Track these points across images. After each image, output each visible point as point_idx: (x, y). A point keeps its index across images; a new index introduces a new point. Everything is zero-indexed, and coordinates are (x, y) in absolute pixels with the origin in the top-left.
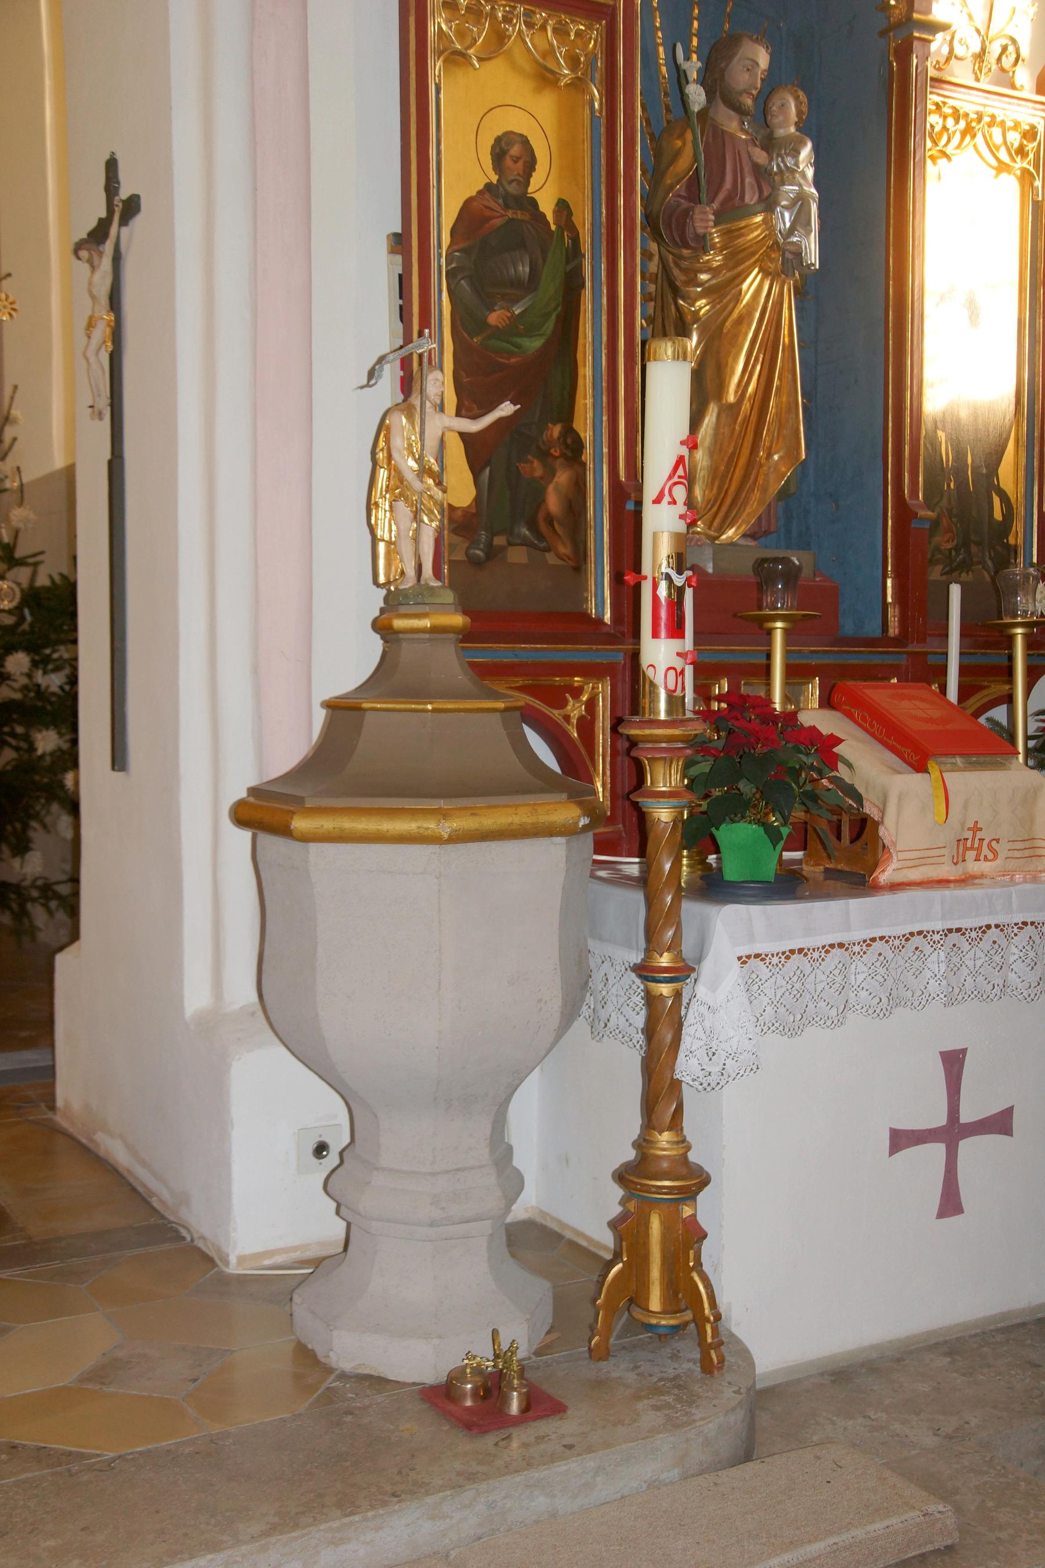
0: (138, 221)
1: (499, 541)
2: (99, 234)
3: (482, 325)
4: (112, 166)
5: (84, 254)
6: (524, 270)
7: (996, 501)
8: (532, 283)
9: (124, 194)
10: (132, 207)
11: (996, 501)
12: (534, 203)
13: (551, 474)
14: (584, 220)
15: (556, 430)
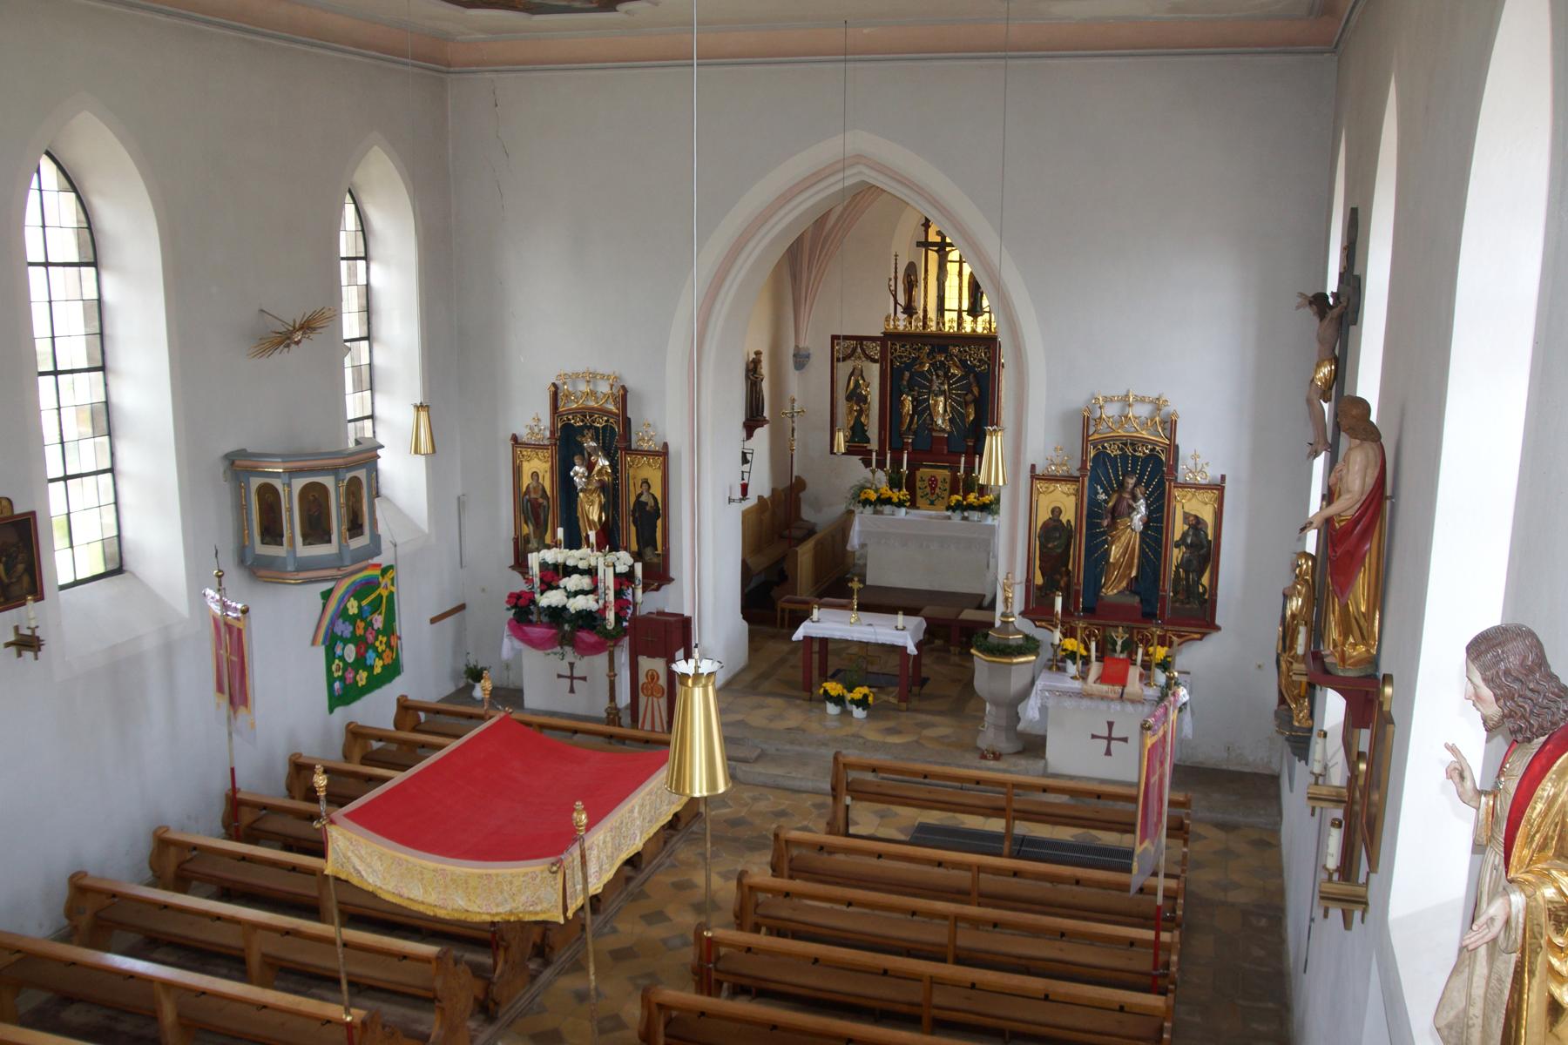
1: (1048, 592)
3: (1046, 547)
6: (1058, 535)
7: (1201, 587)
11: (1201, 587)
12: (1061, 521)
13: (1062, 578)
14: (1073, 523)
15: (1064, 569)
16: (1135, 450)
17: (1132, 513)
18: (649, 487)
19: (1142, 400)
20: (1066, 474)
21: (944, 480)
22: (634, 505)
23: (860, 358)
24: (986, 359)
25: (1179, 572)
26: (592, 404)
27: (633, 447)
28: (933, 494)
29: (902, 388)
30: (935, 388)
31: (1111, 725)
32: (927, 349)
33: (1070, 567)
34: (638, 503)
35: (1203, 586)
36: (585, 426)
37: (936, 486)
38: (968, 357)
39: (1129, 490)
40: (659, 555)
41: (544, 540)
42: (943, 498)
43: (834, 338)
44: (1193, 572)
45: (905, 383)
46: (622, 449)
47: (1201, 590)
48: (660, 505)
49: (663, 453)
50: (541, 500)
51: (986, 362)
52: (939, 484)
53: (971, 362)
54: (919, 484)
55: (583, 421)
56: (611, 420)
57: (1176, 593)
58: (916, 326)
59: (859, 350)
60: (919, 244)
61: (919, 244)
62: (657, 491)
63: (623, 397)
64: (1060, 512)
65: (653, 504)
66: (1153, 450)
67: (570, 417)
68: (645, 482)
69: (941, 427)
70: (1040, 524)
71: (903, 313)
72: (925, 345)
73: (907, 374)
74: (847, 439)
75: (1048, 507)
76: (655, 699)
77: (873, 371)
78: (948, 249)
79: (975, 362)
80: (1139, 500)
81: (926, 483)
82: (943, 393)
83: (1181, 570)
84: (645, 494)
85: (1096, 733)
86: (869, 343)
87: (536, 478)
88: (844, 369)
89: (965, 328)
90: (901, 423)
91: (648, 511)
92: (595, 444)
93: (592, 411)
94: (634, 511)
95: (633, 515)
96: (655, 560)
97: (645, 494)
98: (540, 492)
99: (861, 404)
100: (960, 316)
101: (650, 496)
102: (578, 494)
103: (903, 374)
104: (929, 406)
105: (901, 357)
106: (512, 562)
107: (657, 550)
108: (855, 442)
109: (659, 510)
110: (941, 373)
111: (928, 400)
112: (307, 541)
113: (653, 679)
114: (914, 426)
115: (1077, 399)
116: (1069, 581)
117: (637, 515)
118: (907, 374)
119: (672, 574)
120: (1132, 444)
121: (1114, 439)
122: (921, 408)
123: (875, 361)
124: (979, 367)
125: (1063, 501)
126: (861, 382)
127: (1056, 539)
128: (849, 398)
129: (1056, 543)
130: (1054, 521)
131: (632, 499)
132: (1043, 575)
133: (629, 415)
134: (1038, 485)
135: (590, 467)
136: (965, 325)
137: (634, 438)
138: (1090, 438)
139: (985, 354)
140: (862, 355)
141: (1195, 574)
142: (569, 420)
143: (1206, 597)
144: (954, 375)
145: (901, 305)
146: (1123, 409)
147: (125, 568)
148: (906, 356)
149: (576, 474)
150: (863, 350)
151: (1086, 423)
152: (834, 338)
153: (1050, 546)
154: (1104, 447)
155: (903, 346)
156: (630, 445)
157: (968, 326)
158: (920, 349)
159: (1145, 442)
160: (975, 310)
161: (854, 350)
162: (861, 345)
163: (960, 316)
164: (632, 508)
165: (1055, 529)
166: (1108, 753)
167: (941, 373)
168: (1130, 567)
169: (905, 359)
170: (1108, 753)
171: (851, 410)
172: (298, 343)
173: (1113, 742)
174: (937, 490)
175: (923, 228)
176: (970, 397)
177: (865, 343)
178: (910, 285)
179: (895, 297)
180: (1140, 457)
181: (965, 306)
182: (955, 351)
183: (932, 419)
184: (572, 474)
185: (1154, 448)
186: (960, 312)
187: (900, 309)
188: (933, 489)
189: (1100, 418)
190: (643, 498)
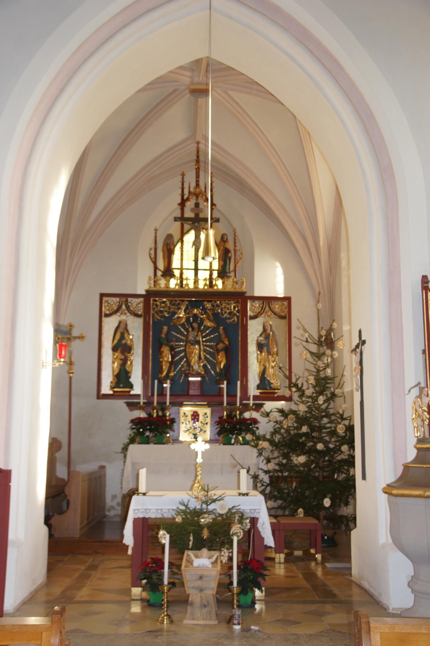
0: (366, 345)
2: (357, 346)
4: (360, 332)
5: (353, 352)
9: (363, 339)
10: (364, 342)
21: (206, 414)
23: (125, 314)
30: (191, 338)
38: (220, 311)
43: (102, 296)
45: (163, 336)
52: (201, 418)
58: (173, 284)
59: (124, 307)
60: (176, 219)
61: (176, 219)
69: (197, 372)
72: (183, 301)
73: (165, 328)
81: (189, 418)
82: (198, 343)
89: (217, 286)
90: (161, 371)
99: (126, 354)
103: (162, 328)
105: (162, 312)
110: (195, 325)
118: (165, 328)
123: (137, 315)
124: (230, 319)
128: (115, 349)
139: (234, 308)
140: (126, 311)
144: (207, 328)
145: (160, 270)
150: (128, 308)
152: (102, 296)
157: (219, 284)
158: (179, 304)
167: (195, 325)
175: (179, 207)
176: (221, 346)
179: (155, 263)
182: (208, 305)
187: (159, 273)
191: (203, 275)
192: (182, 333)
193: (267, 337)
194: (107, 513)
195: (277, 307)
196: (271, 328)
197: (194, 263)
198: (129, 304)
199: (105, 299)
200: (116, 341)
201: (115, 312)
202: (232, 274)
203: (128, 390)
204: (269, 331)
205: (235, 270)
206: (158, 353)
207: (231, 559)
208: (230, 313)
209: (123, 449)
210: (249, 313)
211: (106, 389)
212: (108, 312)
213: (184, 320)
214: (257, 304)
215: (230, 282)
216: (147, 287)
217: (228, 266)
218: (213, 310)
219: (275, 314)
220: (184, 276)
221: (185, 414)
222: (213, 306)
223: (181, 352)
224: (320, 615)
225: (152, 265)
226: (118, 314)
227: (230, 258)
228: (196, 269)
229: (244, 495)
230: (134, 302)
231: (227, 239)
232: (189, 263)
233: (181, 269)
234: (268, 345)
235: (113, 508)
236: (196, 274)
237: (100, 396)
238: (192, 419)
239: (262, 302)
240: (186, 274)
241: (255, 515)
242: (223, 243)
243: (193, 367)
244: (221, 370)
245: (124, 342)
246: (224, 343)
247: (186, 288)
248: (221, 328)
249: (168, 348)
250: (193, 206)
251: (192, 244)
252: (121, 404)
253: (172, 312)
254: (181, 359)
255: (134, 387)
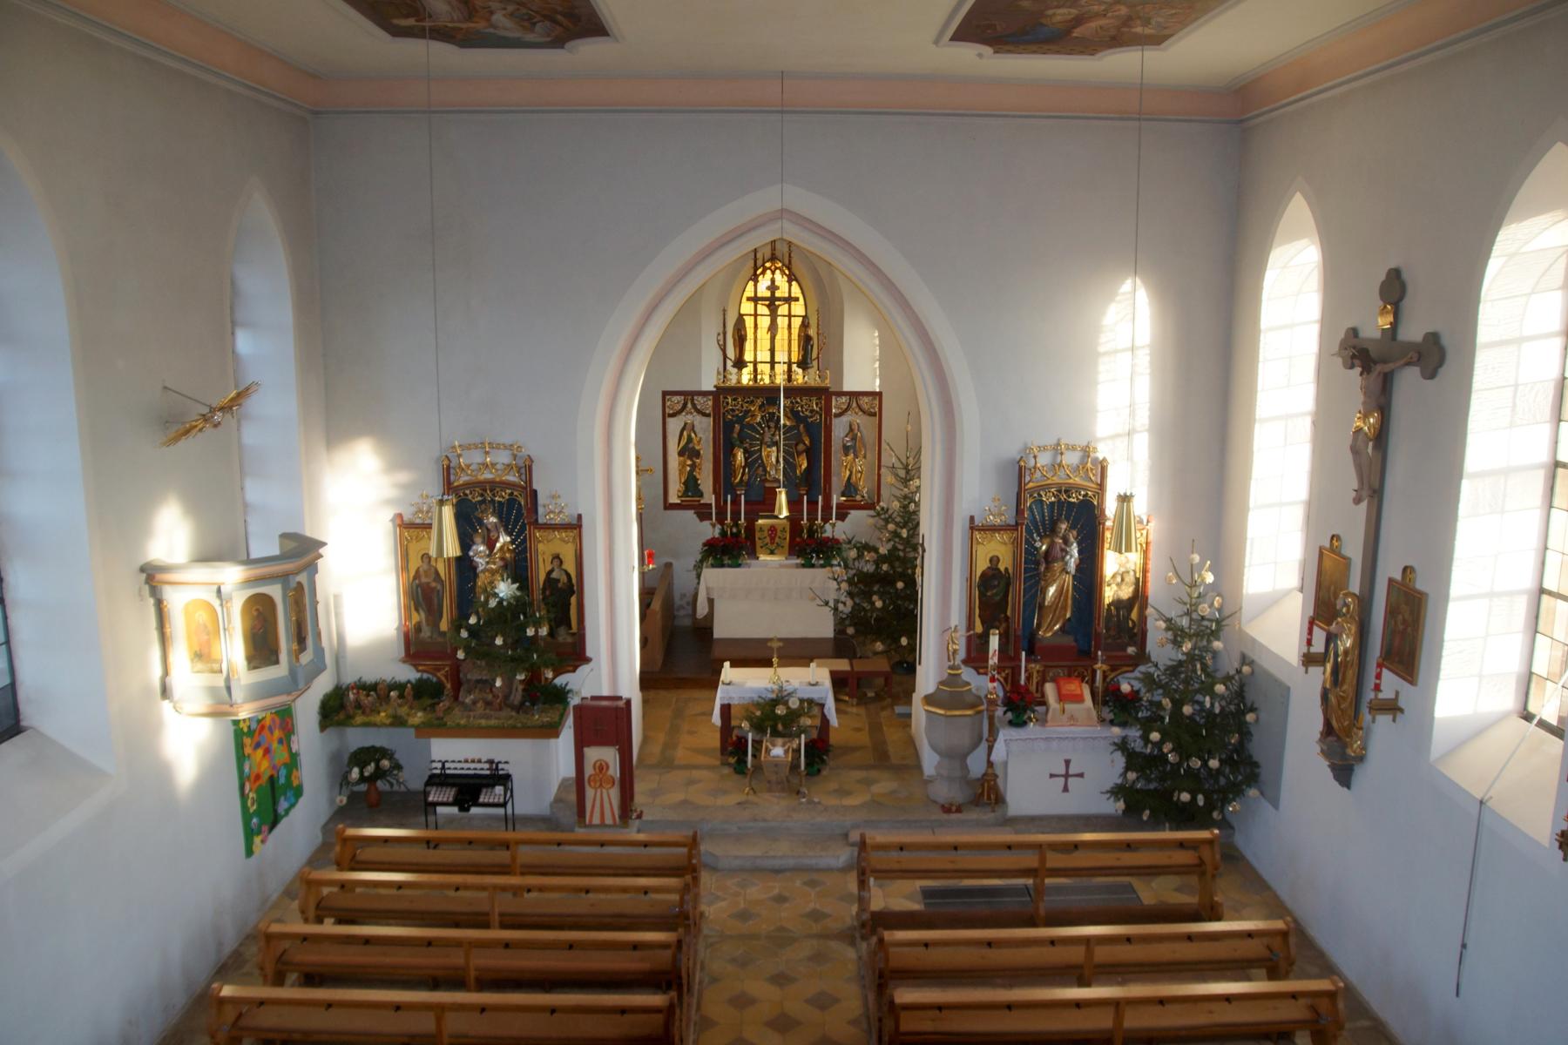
3: (986, 596)
6: (996, 583)
7: (1130, 623)
8: (998, 585)
12: (999, 570)
13: (1001, 624)
14: (1011, 571)
15: (1003, 616)
16: (1069, 497)
17: (1065, 557)
18: (561, 562)
19: (1074, 448)
20: (1003, 524)
21: (784, 529)
22: (544, 583)
23: (691, 413)
24: (818, 409)
25: (1111, 610)
26: (487, 476)
27: (541, 520)
28: (772, 543)
29: (733, 440)
30: (767, 439)
31: (1067, 762)
32: (759, 402)
33: (1009, 613)
34: (550, 581)
35: (1133, 621)
36: (484, 501)
37: (776, 534)
38: (800, 409)
39: (1061, 535)
40: (574, 634)
41: (439, 628)
42: (782, 547)
43: (665, 394)
44: (1123, 608)
45: (735, 435)
46: (530, 524)
47: (1130, 624)
48: (574, 581)
49: (575, 526)
50: (433, 585)
51: (817, 412)
52: (779, 534)
53: (803, 412)
54: (758, 535)
55: (482, 495)
56: (515, 493)
57: (1108, 629)
58: (746, 377)
59: (689, 405)
62: (570, 566)
63: (527, 469)
64: (998, 560)
65: (566, 580)
66: (1086, 495)
67: (468, 492)
68: (557, 558)
70: (979, 574)
71: (734, 366)
74: (680, 494)
75: (986, 555)
76: (604, 790)
77: (704, 429)
78: (777, 303)
79: (807, 413)
80: (1072, 544)
81: (766, 534)
82: (776, 444)
83: (1112, 608)
84: (556, 570)
85: (1054, 772)
86: (700, 398)
87: (426, 560)
88: (675, 425)
91: (561, 588)
92: (495, 520)
93: (493, 485)
94: (544, 589)
95: (544, 592)
96: (569, 640)
97: (556, 570)
98: (433, 576)
99: (694, 459)
100: (790, 370)
101: (563, 573)
102: (476, 575)
104: (760, 457)
105: (733, 410)
106: (403, 654)
107: (570, 628)
108: (689, 496)
109: (573, 586)
110: (772, 424)
111: (760, 450)
112: (252, 665)
113: (601, 768)
114: (746, 477)
115: (1012, 451)
116: (1008, 627)
117: (548, 593)
118: (737, 427)
119: (589, 653)
120: (1066, 491)
121: (1046, 487)
122: (754, 461)
124: (811, 417)
125: (998, 550)
126: (693, 435)
127: (995, 587)
128: (681, 454)
129: (994, 591)
130: (993, 569)
131: (542, 577)
132: (983, 623)
133: (535, 486)
134: (977, 535)
135: (491, 544)
136: (729, 376)
137: (541, 510)
138: (1026, 487)
139: (817, 404)
140: (693, 411)
141: (1125, 610)
142: (466, 495)
143: (1135, 631)
146: (1055, 457)
147: (24, 723)
148: (738, 410)
149: (477, 553)
150: (694, 406)
151: (1021, 472)
152: (665, 394)
153: (989, 594)
154: (1040, 495)
155: (735, 400)
156: (537, 520)
157: (799, 377)
158: (752, 401)
159: (1078, 488)
160: (804, 364)
161: (685, 405)
162: (692, 400)
163: (790, 370)
164: (541, 586)
165: (994, 577)
166: (1066, 789)
167: (772, 424)
168: (1064, 608)
169: (737, 412)
170: (1066, 789)
171: (683, 465)
172: (216, 425)
173: (1070, 780)
174: (777, 540)
176: (801, 447)
177: (695, 398)
178: (740, 340)
180: (1074, 503)
181: (794, 359)
183: (765, 470)
184: (471, 554)
185: (1087, 494)
186: (790, 364)
188: (772, 539)
189: (1035, 467)
190: (554, 575)
191: (781, 369)
192: (758, 433)
193: (854, 439)
194: (676, 613)
195: (865, 400)
196: (859, 427)
197: (769, 353)
198: (696, 402)
199: (668, 397)
200: (682, 444)
201: (680, 412)
202: (815, 363)
203: (698, 499)
204: (856, 431)
205: (818, 358)
206: (730, 453)
207: (800, 744)
208: (812, 411)
209: (695, 566)
210: (834, 411)
211: (674, 499)
212: (671, 412)
213: (758, 419)
214: (844, 399)
215: (813, 371)
216: (715, 383)
217: (809, 356)
218: (793, 408)
219: (864, 412)
220: (759, 371)
221: (761, 528)
222: (792, 402)
223: (755, 452)
224: (868, 783)
225: (721, 353)
226: (684, 413)
227: (812, 346)
228: (773, 363)
229: (813, 685)
230: (699, 400)
231: (808, 323)
232: (764, 355)
233: (755, 363)
234: (854, 447)
235: (682, 607)
236: (772, 368)
237: (669, 507)
238: (770, 535)
239: (848, 397)
240: (760, 367)
241: (823, 702)
242: (804, 329)
243: (769, 473)
244: (801, 474)
245: (691, 445)
246: (804, 444)
247: (762, 383)
248: (802, 426)
249: (742, 450)
250: (769, 283)
251: (766, 330)
252: (690, 515)
253: (745, 411)
254: (756, 460)
255: (705, 495)
